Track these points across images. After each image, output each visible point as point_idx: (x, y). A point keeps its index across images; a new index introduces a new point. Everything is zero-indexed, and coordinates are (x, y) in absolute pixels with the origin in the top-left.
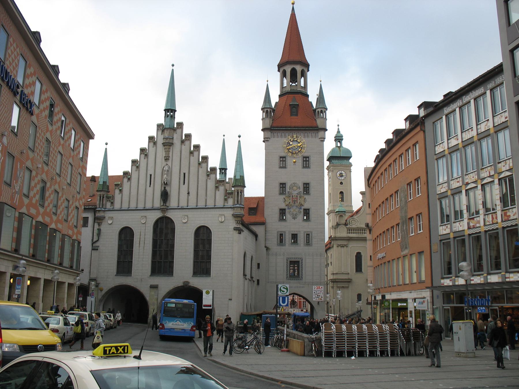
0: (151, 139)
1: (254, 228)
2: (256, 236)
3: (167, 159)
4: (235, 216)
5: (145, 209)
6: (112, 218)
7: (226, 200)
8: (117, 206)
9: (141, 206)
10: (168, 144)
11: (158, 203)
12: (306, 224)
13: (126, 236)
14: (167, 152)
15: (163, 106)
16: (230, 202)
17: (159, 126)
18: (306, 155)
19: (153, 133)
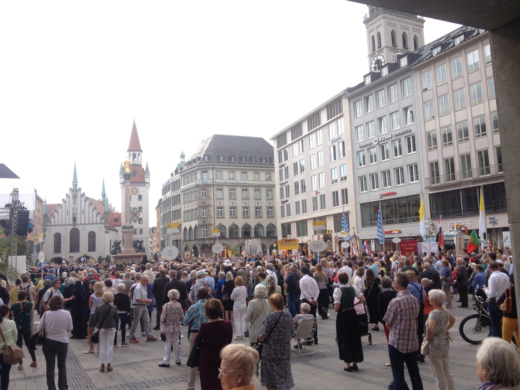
0: (67, 195)
1: (116, 228)
2: (117, 231)
3: (75, 203)
4: (105, 227)
5: (65, 225)
6: (50, 229)
7: (101, 220)
8: (52, 223)
9: (64, 223)
10: (75, 197)
11: (71, 222)
12: (140, 225)
13: (58, 237)
14: (75, 201)
15: (72, 180)
16: (103, 221)
17: (70, 189)
18: (140, 194)
19: (68, 192)
